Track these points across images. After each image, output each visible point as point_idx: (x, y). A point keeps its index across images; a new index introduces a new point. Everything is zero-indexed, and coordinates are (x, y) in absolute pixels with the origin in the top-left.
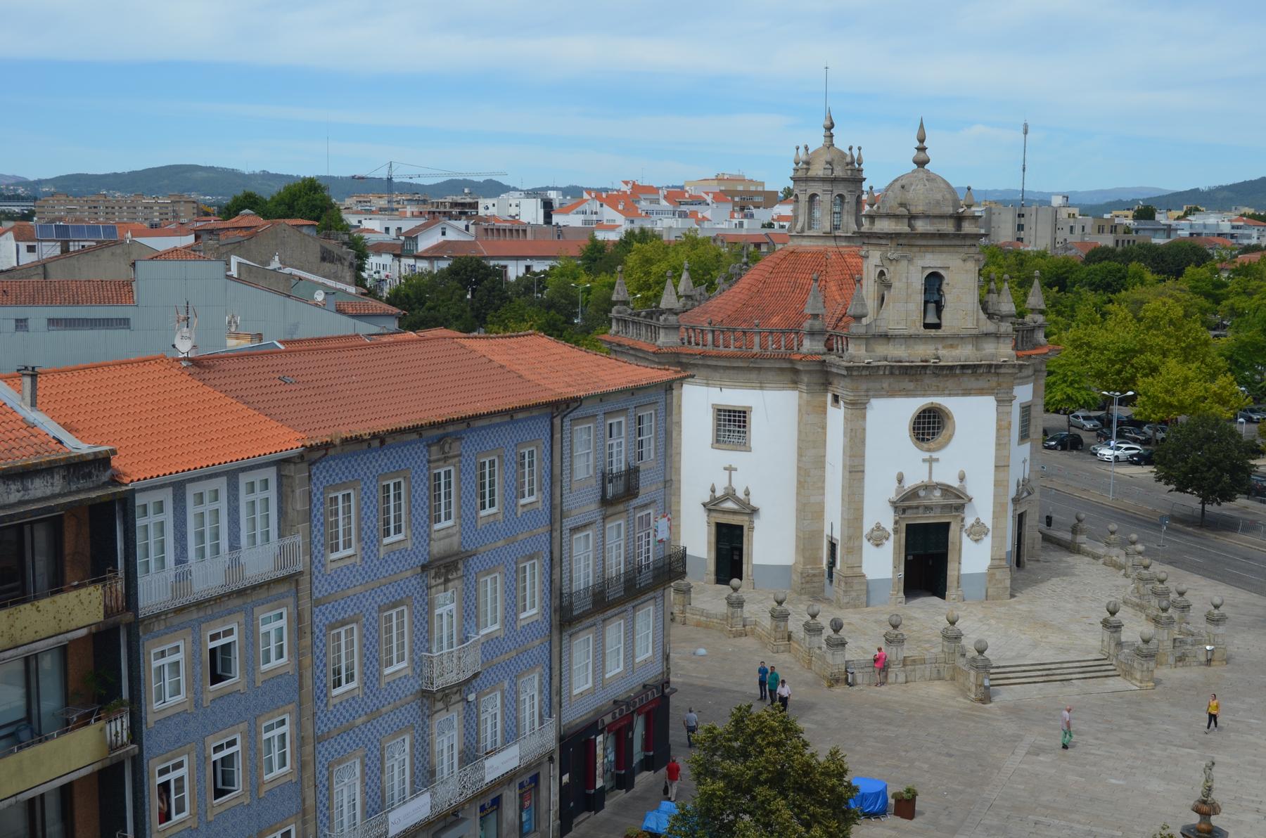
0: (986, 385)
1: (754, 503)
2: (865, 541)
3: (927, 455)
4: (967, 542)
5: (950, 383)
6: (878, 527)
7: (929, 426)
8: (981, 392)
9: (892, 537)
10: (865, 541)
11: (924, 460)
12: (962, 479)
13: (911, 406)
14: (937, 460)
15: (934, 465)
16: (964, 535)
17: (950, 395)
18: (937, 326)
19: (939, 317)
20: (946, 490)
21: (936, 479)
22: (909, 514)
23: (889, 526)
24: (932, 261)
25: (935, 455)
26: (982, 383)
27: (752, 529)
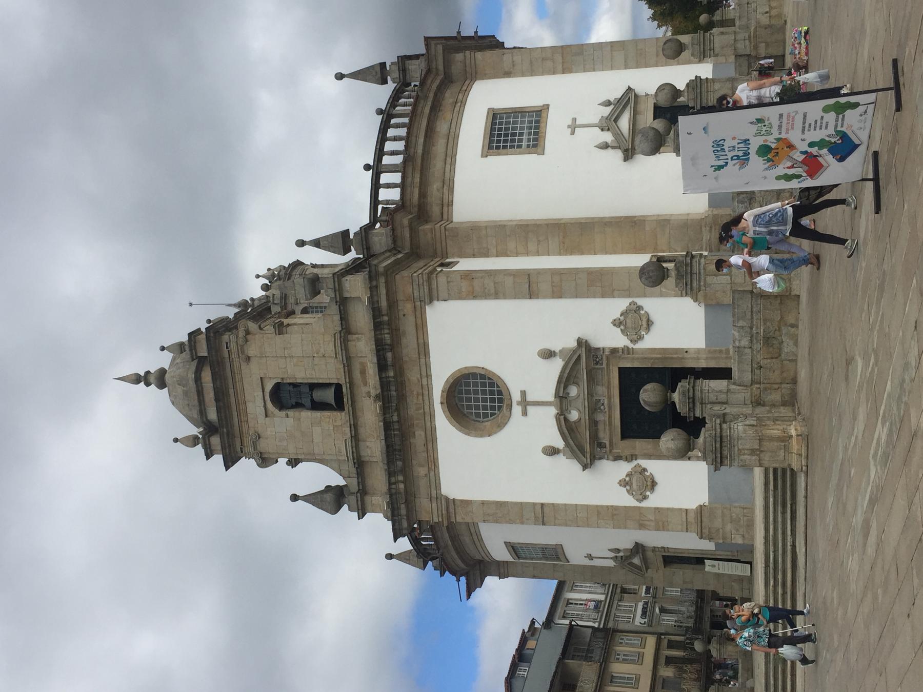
0: (411, 319)
1: (630, 546)
2: (645, 504)
3: (517, 410)
4: (653, 341)
5: (412, 375)
6: (624, 483)
8: (421, 327)
9: (644, 463)
10: (645, 504)
11: (525, 413)
12: (548, 354)
13: (447, 433)
14: (523, 393)
15: (530, 398)
16: (640, 345)
17: (429, 376)
18: (338, 387)
19: (328, 385)
20: (565, 380)
21: (551, 397)
22: (604, 437)
23: (623, 468)
24: (255, 403)
25: (516, 397)
26: (408, 324)
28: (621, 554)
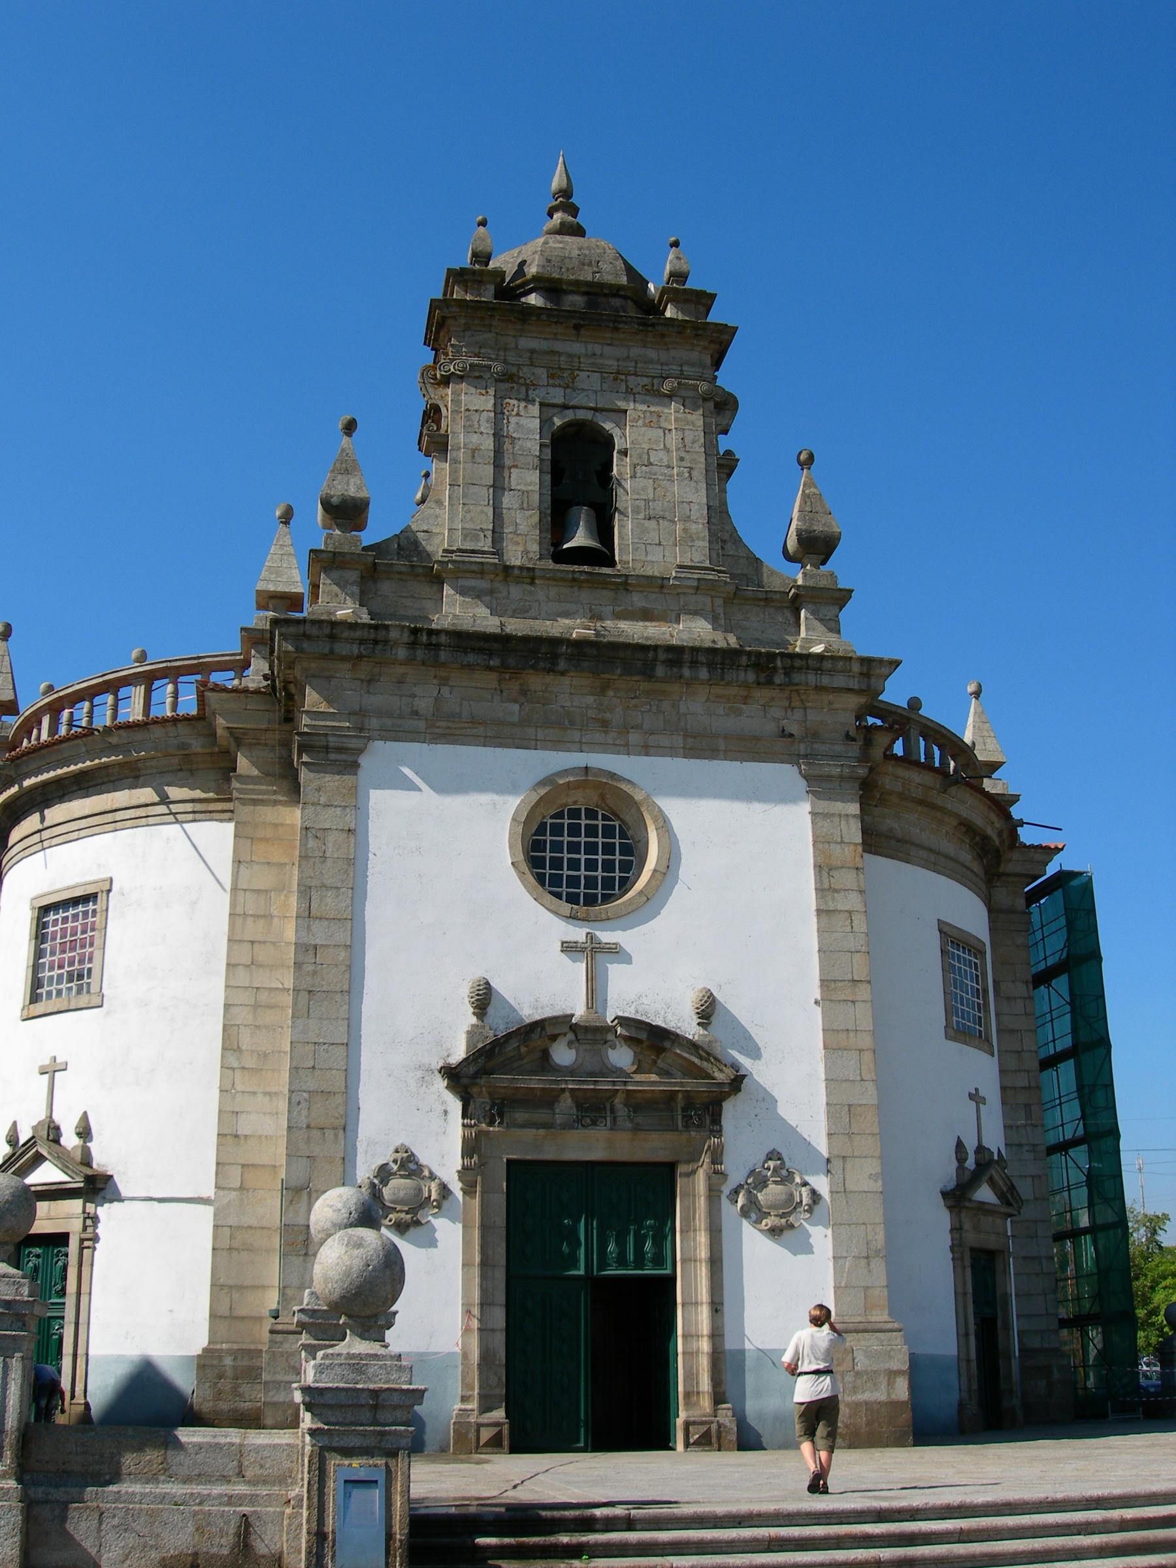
3: (578, 933)
7: (585, 857)
11: (568, 948)
17: (646, 750)
27: (90, 1240)
28: (70, 1140)
